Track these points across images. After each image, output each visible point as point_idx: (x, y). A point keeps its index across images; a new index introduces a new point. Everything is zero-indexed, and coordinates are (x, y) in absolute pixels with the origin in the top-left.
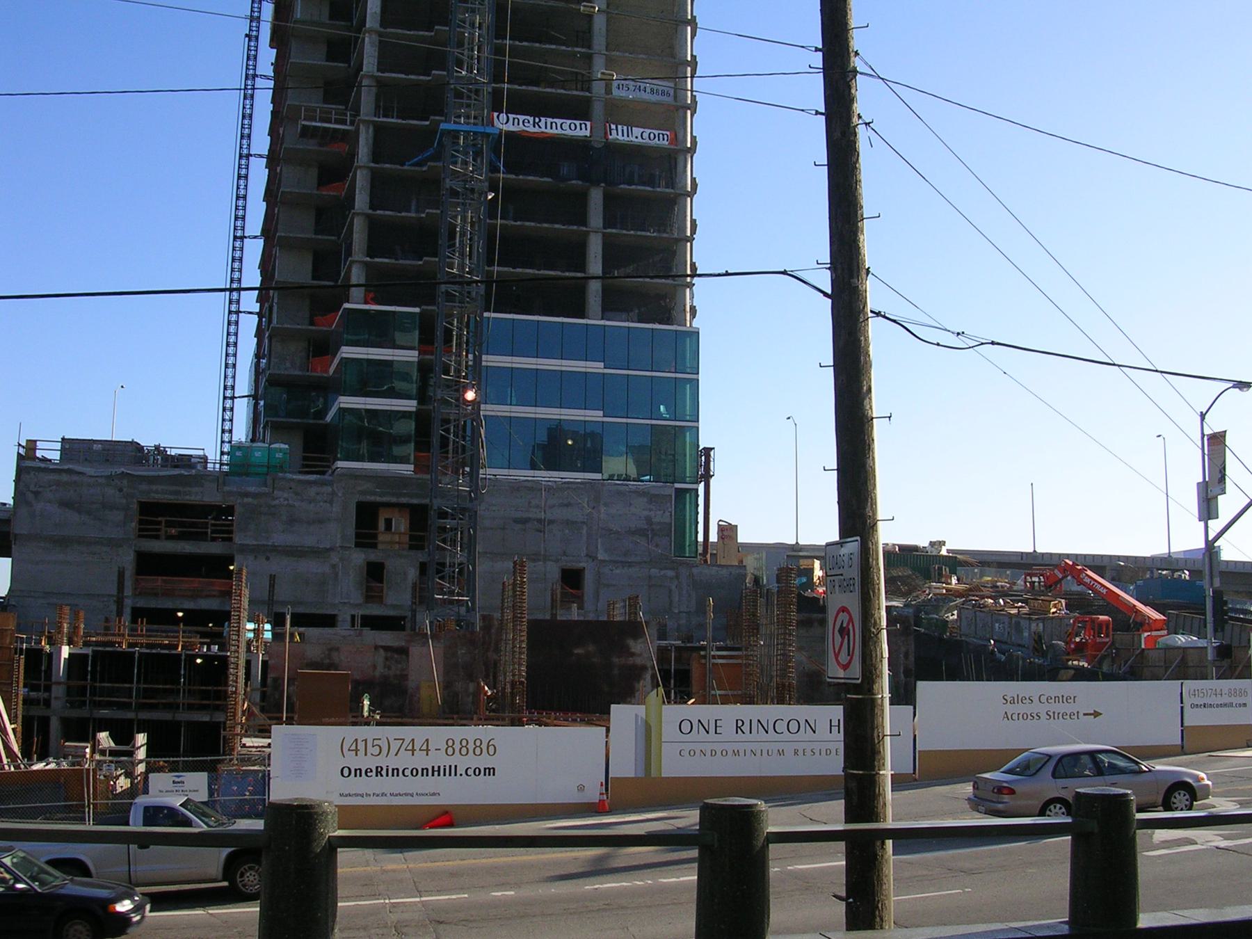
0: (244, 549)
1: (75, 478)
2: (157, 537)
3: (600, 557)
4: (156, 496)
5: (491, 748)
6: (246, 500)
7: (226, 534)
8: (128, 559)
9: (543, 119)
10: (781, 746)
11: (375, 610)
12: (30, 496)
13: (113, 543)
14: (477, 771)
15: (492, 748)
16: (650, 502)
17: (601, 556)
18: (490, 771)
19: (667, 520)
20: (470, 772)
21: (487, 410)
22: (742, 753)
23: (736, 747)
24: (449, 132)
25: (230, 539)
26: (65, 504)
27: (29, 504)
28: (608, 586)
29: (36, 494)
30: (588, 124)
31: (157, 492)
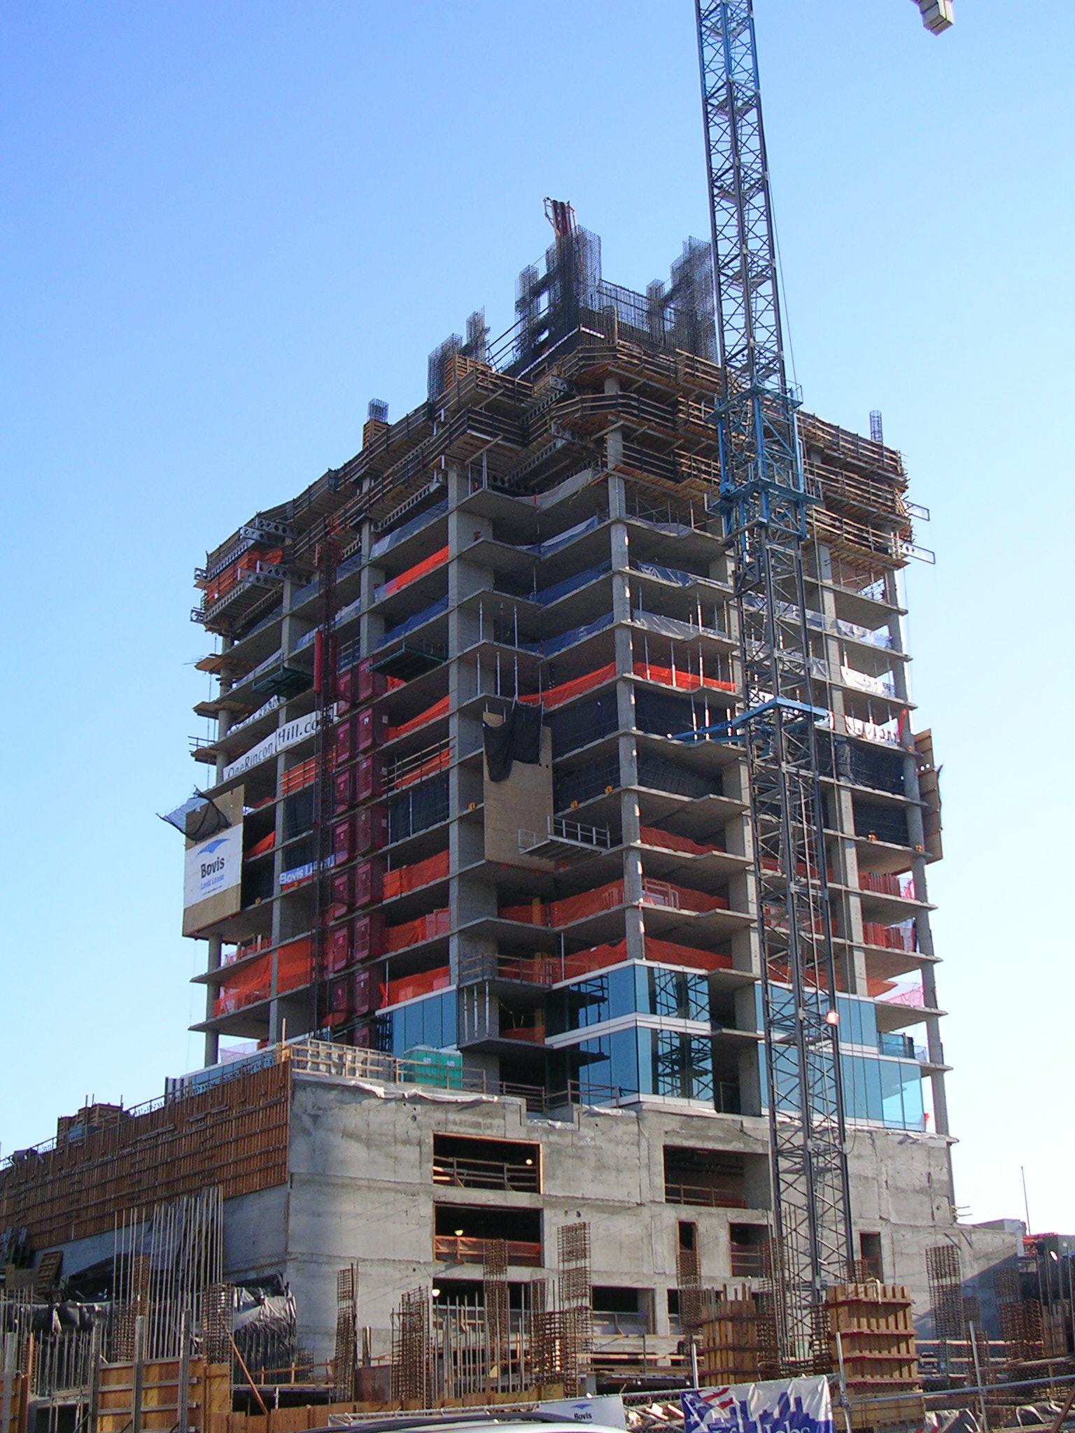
0: (554, 1202)
4: (456, 1128)
7: (529, 1182)
8: (428, 1211)
13: (412, 1193)
25: (536, 1189)
31: (455, 1123)
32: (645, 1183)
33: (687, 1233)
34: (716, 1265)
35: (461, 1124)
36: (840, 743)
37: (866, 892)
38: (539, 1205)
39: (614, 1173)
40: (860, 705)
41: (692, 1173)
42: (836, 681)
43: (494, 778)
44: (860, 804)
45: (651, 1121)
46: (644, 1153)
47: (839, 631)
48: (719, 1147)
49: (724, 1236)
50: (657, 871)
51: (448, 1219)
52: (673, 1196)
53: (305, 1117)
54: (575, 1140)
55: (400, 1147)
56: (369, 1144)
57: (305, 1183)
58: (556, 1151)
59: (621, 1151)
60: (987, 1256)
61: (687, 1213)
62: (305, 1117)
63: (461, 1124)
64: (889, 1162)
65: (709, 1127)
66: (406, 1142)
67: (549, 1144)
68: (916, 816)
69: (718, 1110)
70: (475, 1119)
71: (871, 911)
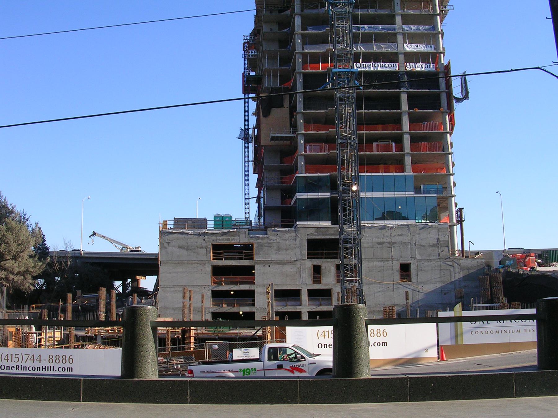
0: (259, 263)
2: (222, 259)
3: (418, 257)
5: (385, 334)
6: (258, 241)
8: (209, 269)
9: (376, 63)
10: (518, 328)
11: (317, 286)
12: (166, 245)
13: (202, 263)
14: (379, 344)
15: (385, 334)
16: (439, 231)
17: (418, 257)
18: (385, 344)
19: (447, 240)
20: (376, 344)
21: (362, 195)
22: (500, 332)
23: (497, 329)
24: (336, 72)
25: (252, 259)
26: (180, 247)
27: (166, 248)
28: (421, 270)
29: (168, 243)
30: (397, 64)
31: (220, 240)
32: (298, 253)
33: (317, 270)
34: (329, 280)
35: (222, 240)
36: (401, 75)
37: (412, 131)
38: (253, 264)
39: (285, 251)
40: (412, 57)
41: (318, 248)
42: (401, 50)
43: (264, 116)
44: (411, 97)
45: (302, 231)
46: (298, 243)
47: (403, 30)
48: (333, 237)
49: (333, 269)
50: (309, 140)
51: (217, 272)
52: (310, 256)
54: (269, 241)
56: (187, 250)
57: (165, 263)
58: (261, 245)
59: (287, 242)
60: (468, 269)
61: (316, 262)
63: (222, 240)
64: (417, 236)
65: (328, 231)
66: (201, 248)
67: (258, 243)
68: (444, 97)
69: (332, 224)
70: (228, 237)
71: (415, 139)
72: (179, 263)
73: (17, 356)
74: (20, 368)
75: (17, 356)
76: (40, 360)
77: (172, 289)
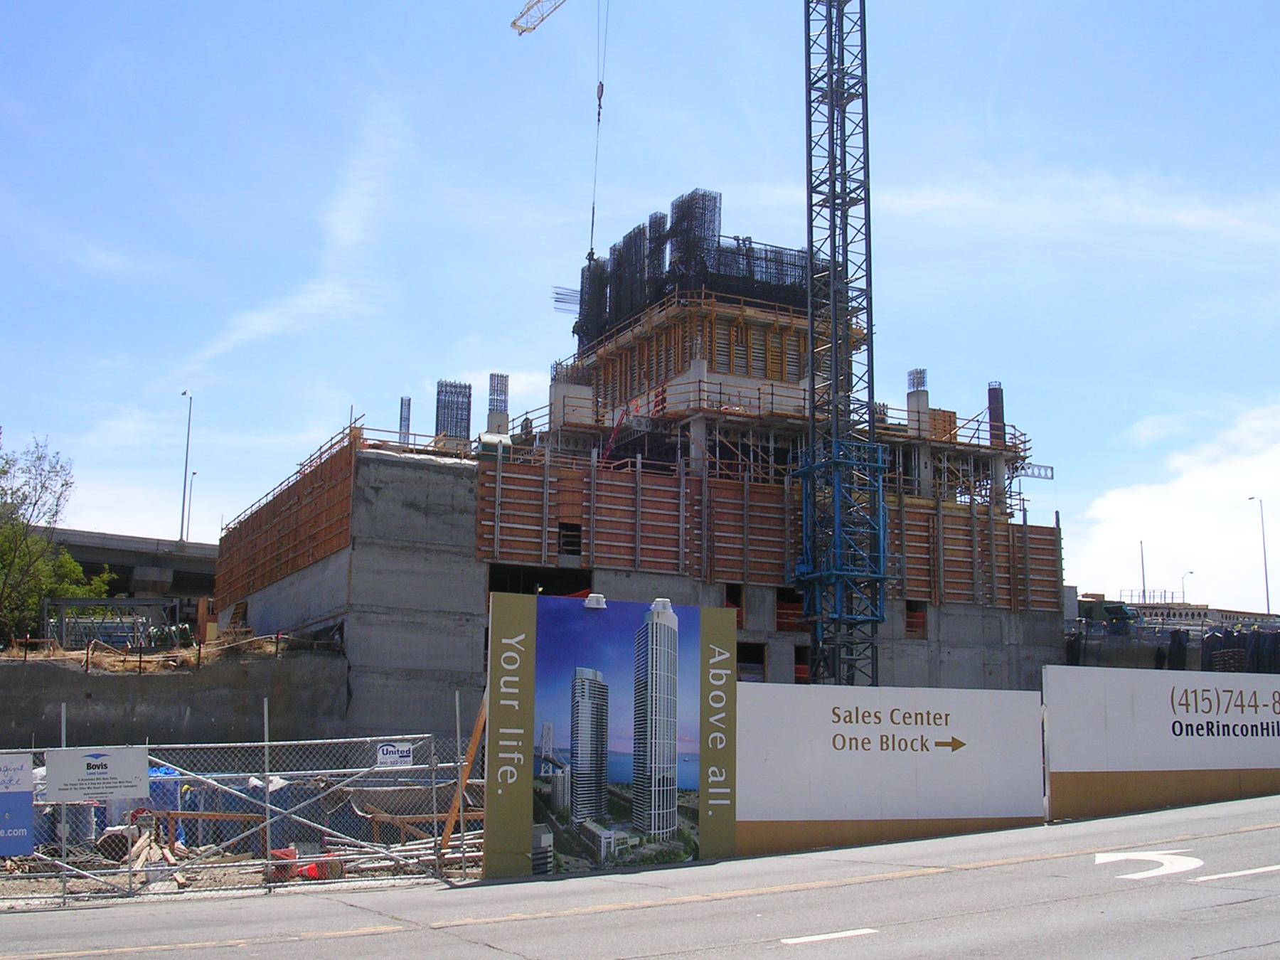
1: (420, 473)
26: (411, 505)
27: (368, 502)
29: (377, 490)
53: (367, 490)
55: (456, 515)
56: (427, 511)
62: (367, 490)
66: (462, 512)
72: (403, 548)
73: (1206, 695)
74: (1215, 730)
75: (1206, 695)
76: (1256, 706)
77: (384, 618)
